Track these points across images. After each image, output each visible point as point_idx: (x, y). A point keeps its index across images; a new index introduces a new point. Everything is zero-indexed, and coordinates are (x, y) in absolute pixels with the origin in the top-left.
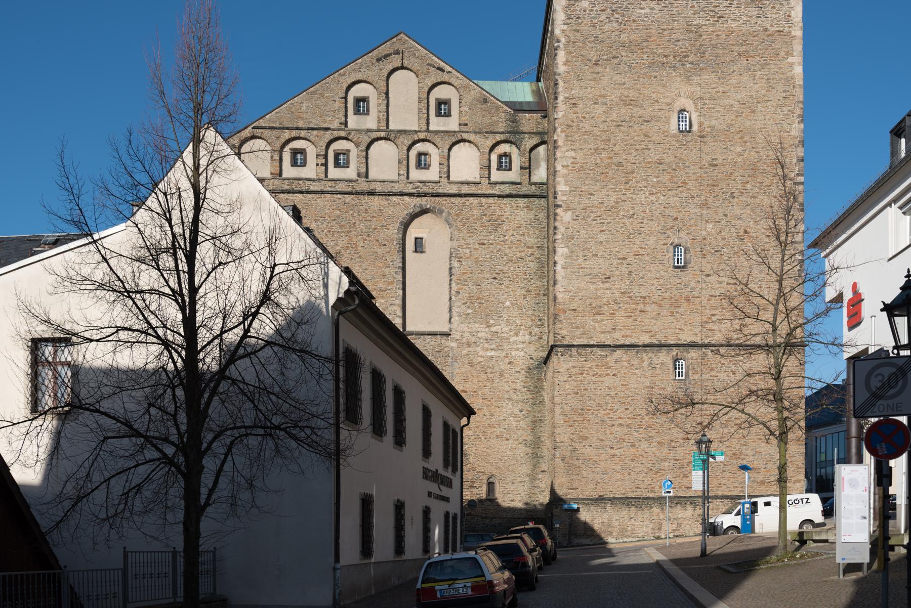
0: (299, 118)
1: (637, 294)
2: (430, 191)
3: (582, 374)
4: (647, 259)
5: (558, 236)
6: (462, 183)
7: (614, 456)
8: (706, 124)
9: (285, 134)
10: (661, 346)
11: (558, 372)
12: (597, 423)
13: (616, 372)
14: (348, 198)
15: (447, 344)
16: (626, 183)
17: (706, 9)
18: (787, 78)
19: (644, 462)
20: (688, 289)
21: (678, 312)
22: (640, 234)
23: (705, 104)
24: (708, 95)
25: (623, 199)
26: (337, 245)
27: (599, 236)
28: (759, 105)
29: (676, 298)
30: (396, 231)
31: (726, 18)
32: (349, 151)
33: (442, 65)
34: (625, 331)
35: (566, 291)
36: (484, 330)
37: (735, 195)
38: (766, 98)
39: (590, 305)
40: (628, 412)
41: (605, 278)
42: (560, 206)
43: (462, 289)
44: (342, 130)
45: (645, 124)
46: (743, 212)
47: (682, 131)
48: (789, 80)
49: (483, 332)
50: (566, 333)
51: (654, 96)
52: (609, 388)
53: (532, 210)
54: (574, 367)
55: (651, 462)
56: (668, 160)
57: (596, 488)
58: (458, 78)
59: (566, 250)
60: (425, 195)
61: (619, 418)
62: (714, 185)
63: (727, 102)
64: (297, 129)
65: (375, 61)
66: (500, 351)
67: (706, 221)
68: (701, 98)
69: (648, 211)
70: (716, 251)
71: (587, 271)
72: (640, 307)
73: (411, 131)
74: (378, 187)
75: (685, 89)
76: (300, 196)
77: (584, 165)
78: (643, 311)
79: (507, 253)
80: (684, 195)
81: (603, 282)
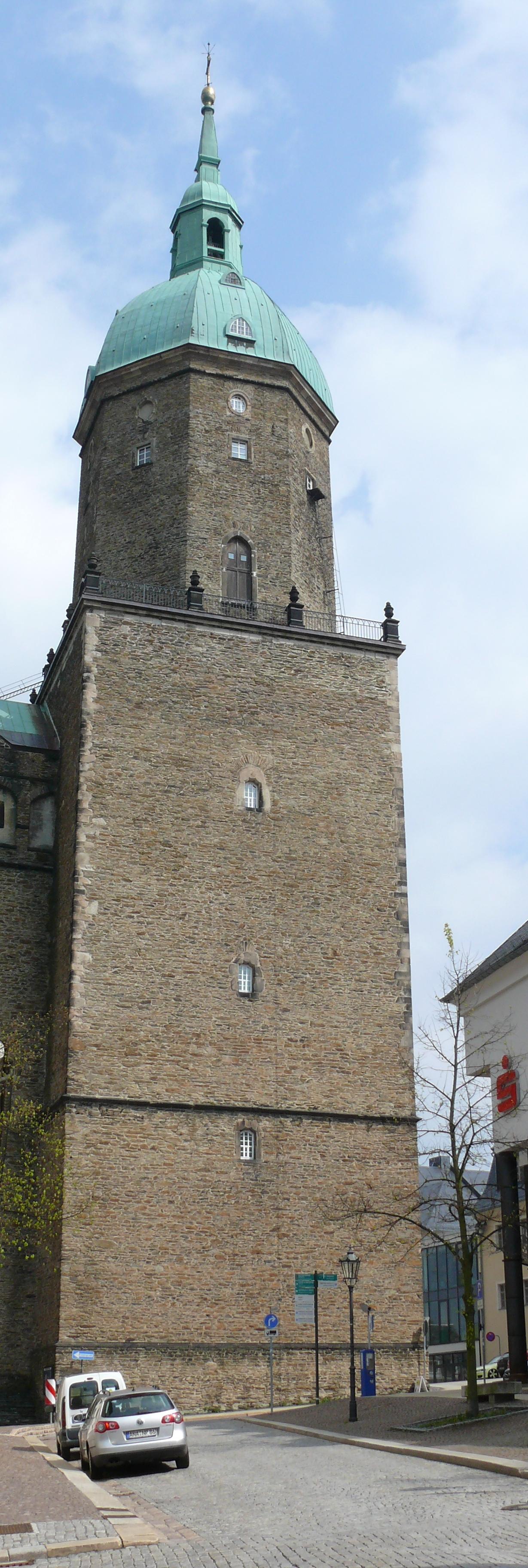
3: (106, 1143)
5: (77, 936)
8: (282, 803)
10: (220, 1110)
11: (71, 1139)
12: (127, 1222)
19: (195, 1287)
21: (244, 1061)
22: (193, 942)
25: (170, 891)
27: (136, 939)
28: (348, 788)
31: (306, 673)
34: (171, 1082)
39: (121, 1039)
40: (173, 1206)
41: (143, 1003)
42: (82, 892)
47: (250, 809)
51: (214, 757)
52: (146, 1168)
53: (31, 887)
54: (95, 1132)
55: (206, 1287)
59: (88, 957)
61: (159, 1215)
62: (292, 886)
68: (275, 769)
69: (204, 912)
72: (193, 1048)
75: (253, 753)
77: (118, 839)
80: (254, 894)
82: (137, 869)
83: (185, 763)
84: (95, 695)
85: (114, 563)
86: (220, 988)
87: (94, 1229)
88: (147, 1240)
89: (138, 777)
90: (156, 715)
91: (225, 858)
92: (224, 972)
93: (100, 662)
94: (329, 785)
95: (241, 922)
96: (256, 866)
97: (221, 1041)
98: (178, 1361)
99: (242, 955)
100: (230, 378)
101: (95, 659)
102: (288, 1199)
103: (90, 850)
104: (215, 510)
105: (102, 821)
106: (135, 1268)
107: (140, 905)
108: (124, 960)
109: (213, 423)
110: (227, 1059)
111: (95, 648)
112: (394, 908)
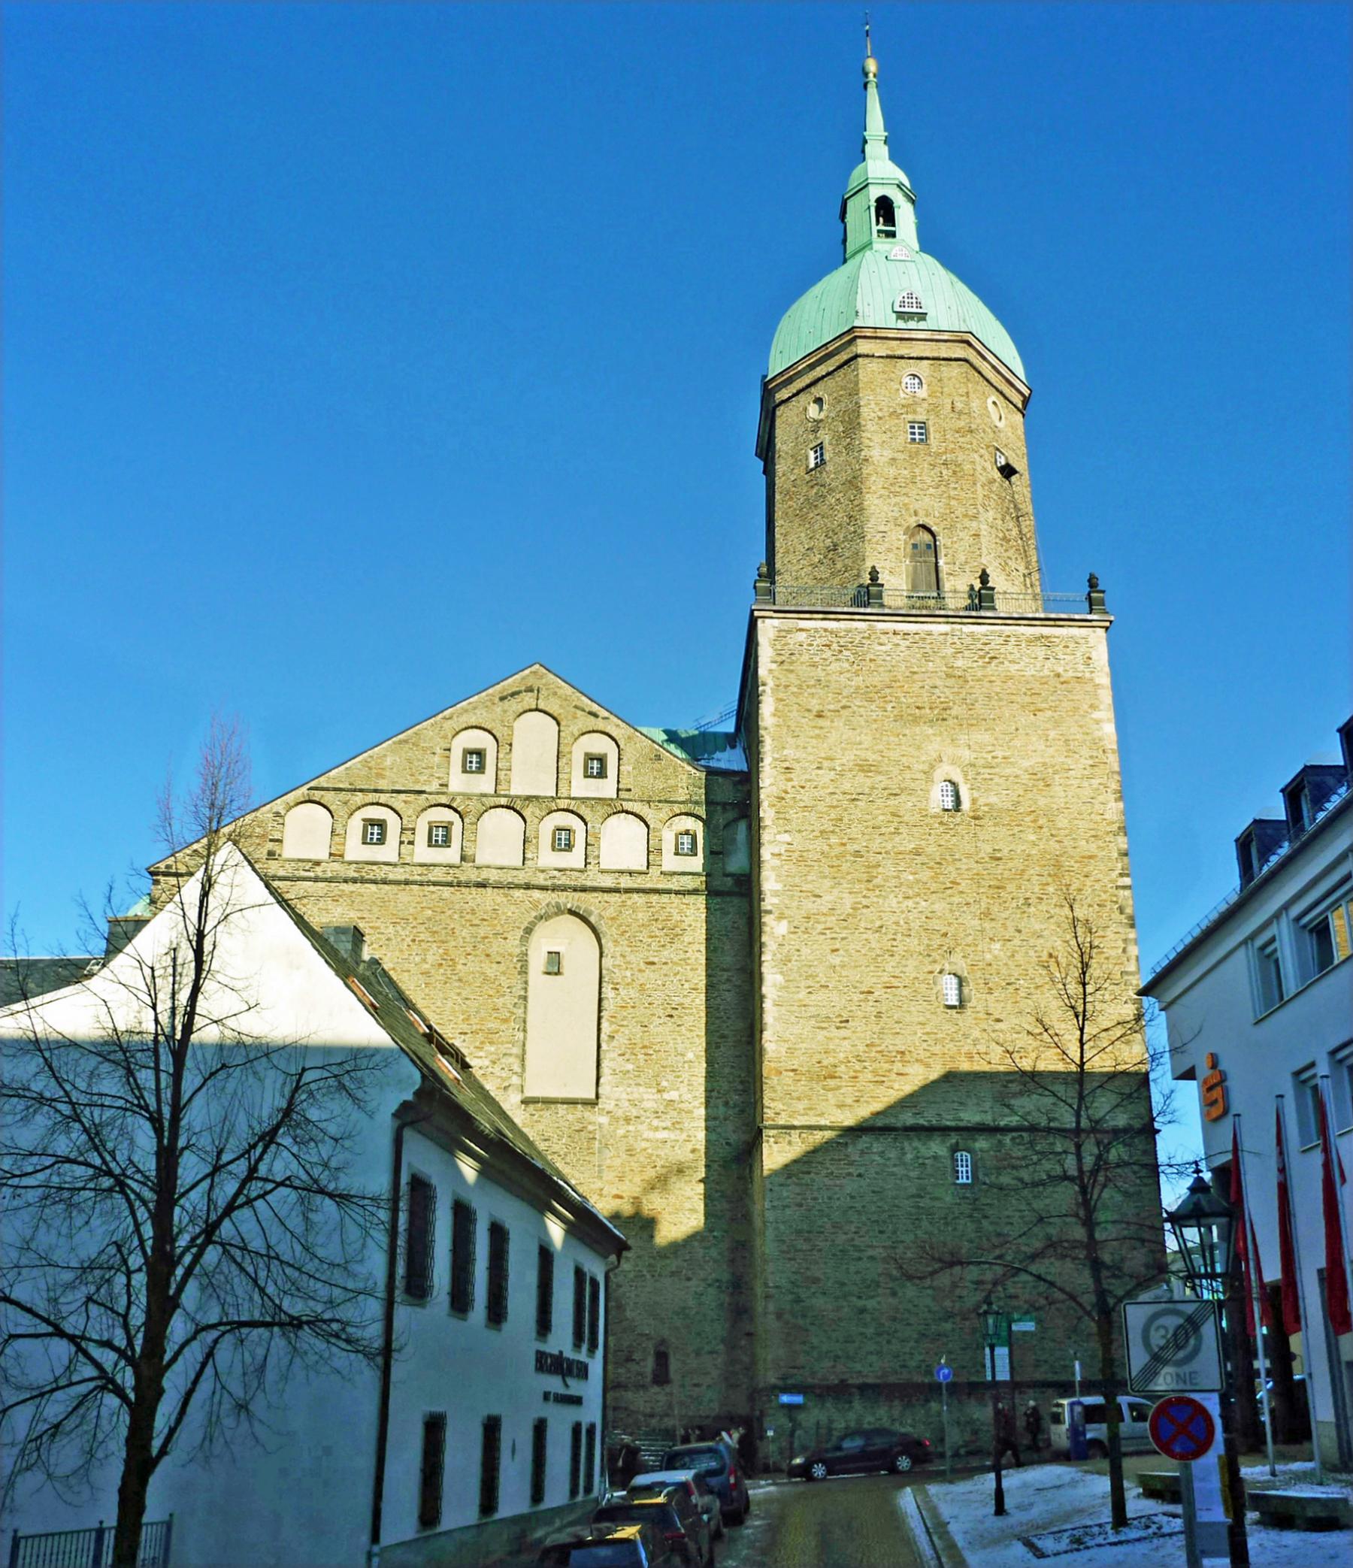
0: (380, 776)
1: (891, 1048)
2: (572, 883)
6: (622, 872)
7: (863, 1311)
8: (982, 801)
9: (357, 798)
13: (862, 1170)
14: (446, 892)
15: (592, 1118)
16: (868, 881)
17: (972, 647)
18: (1094, 739)
20: (969, 1041)
22: (892, 955)
23: (978, 774)
24: (982, 762)
25: (865, 903)
26: (424, 961)
27: (829, 957)
28: (1057, 776)
29: (951, 1053)
30: (518, 942)
32: (451, 823)
33: (595, 708)
35: (781, 1039)
36: (651, 1097)
37: (1030, 901)
38: (1066, 767)
39: (819, 1062)
40: (884, 1236)
41: (841, 1022)
42: (769, 912)
43: (617, 1032)
44: (443, 793)
45: (892, 798)
46: (1043, 927)
48: (1096, 742)
49: (650, 1099)
50: (782, 1107)
51: (904, 759)
52: (852, 1197)
56: (930, 850)
57: (834, 1367)
58: (618, 726)
59: (780, 978)
60: (564, 888)
62: (998, 888)
63: (1008, 771)
64: (376, 791)
65: (497, 700)
66: (678, 1132)
67: (991, 939)
70: (1008, 984)
71: (813, 1010)
73: (546, 797)
74: (493, 876)
76: (373, 887)
77: (804, 854)
78: (901, 1074)
79: (689, 978)
80: (956, 899)
81: (838, 1028)
82: (828, 883)
83: (873, 768)
84: (772, 709)
85: (794, 574)
87: (799, 1264)
88: (857, 1272)
89: (823, 788)
90: (839, 723)
93: (776, 674)
94: (1034, 777)
98: (896, 1403)
99: (947, 965)
100: (902, 357)
101: (771, 671)
102: (1012, 1224)
103: (773, 869)
104: (894, 500)
105: (786, 837)
106: (845, 1304)
107: (831, 921)
108: (818, 979)
109: (886, 409)
111: (769, 660)
112: (1116, 902)
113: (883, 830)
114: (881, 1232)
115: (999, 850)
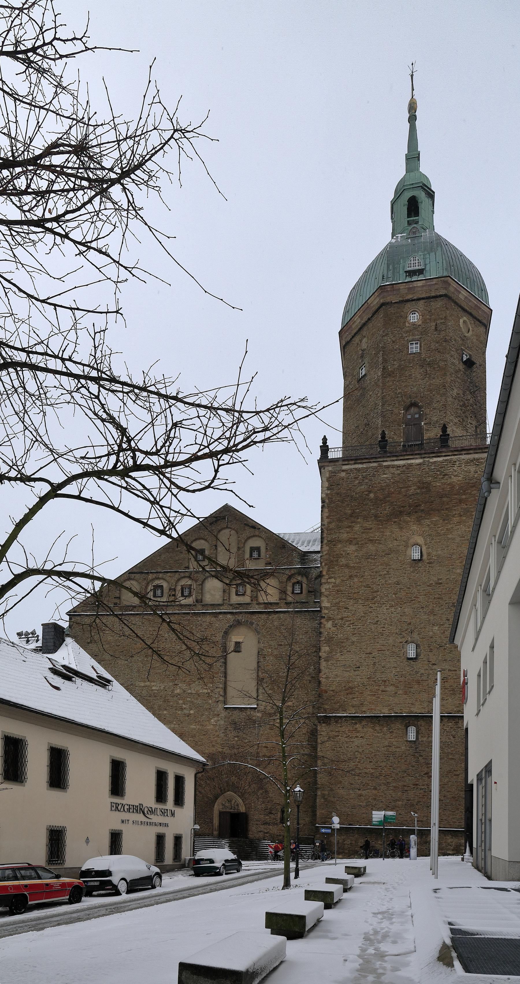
4: (387, 653)
7: (361, 795)
21: (410, 692)
22: (382, 635)
40: (372, 764)
61: (365, 768)
69: (388, 619)
86: (397, 656)
91: (400, 589)
92: (399, 648)
95: (409, 621)
96: (418, 590)
97: (398, 683)
110: (400, 692)
113: (381, 573)
114: (370, 762)
115: (441, 579)
